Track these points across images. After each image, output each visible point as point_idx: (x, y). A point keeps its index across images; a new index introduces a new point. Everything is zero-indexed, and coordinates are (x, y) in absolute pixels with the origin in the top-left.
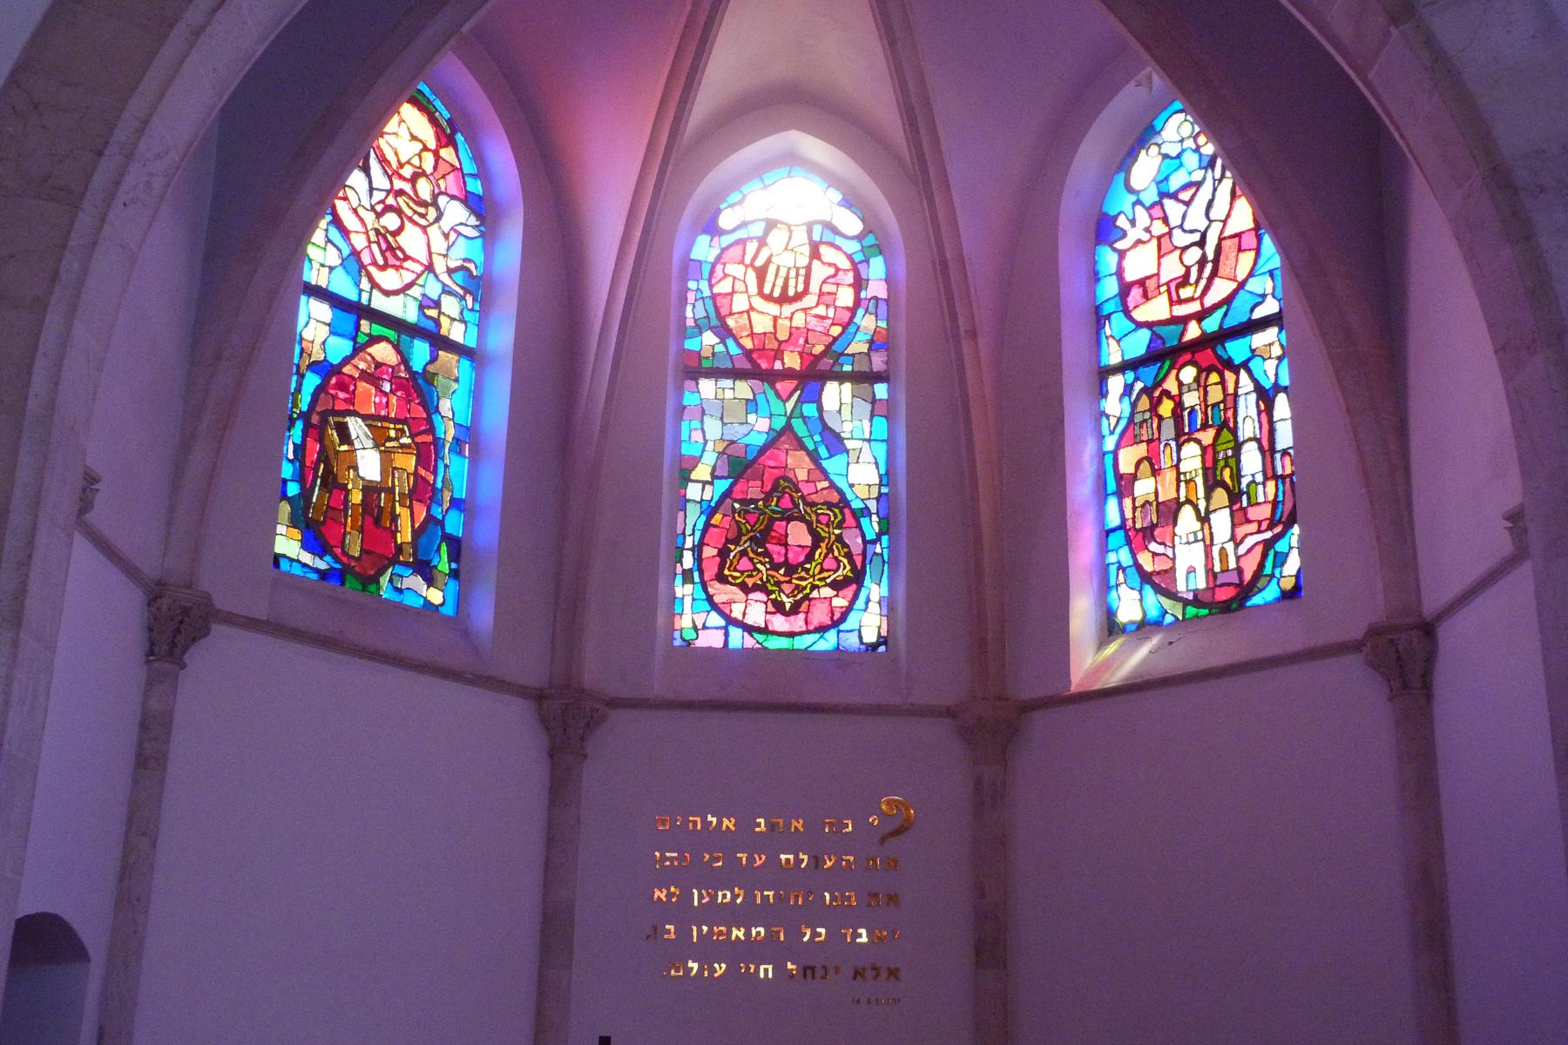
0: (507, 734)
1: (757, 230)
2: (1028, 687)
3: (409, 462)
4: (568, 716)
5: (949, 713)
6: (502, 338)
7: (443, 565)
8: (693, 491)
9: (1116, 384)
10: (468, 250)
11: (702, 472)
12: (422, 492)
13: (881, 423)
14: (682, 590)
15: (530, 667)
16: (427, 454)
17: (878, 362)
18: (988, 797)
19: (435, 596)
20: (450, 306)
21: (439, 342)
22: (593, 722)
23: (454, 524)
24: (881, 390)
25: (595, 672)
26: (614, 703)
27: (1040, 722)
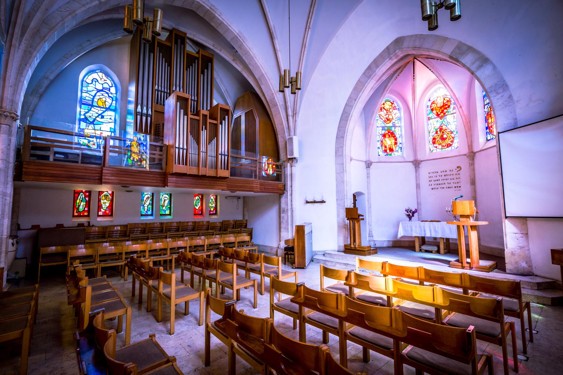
0: (411, 166)
1: (436, 99)
2: (475, 150)
3: (394, 141)
4: (417, 163)
5: (465, 155)
6: (403, 124)
7: (399, 150)
8: (431, 134)
9: (486, 107)
10: (398, 115)
11: (431, 132)
12: (396, 143)
13: (455, 120)
14: (431, 146)
15: (412, 159)
16: (396, 140)
17: (454, 111)
18: (472, 164)
19: (399, 154)
20: (396, 122)
21: (395, 127)
22: (419, 164)
23: (400, 146)
24: (455, 115)
25: (420, 157)
26: (422, 161)
27: (477, 154)
